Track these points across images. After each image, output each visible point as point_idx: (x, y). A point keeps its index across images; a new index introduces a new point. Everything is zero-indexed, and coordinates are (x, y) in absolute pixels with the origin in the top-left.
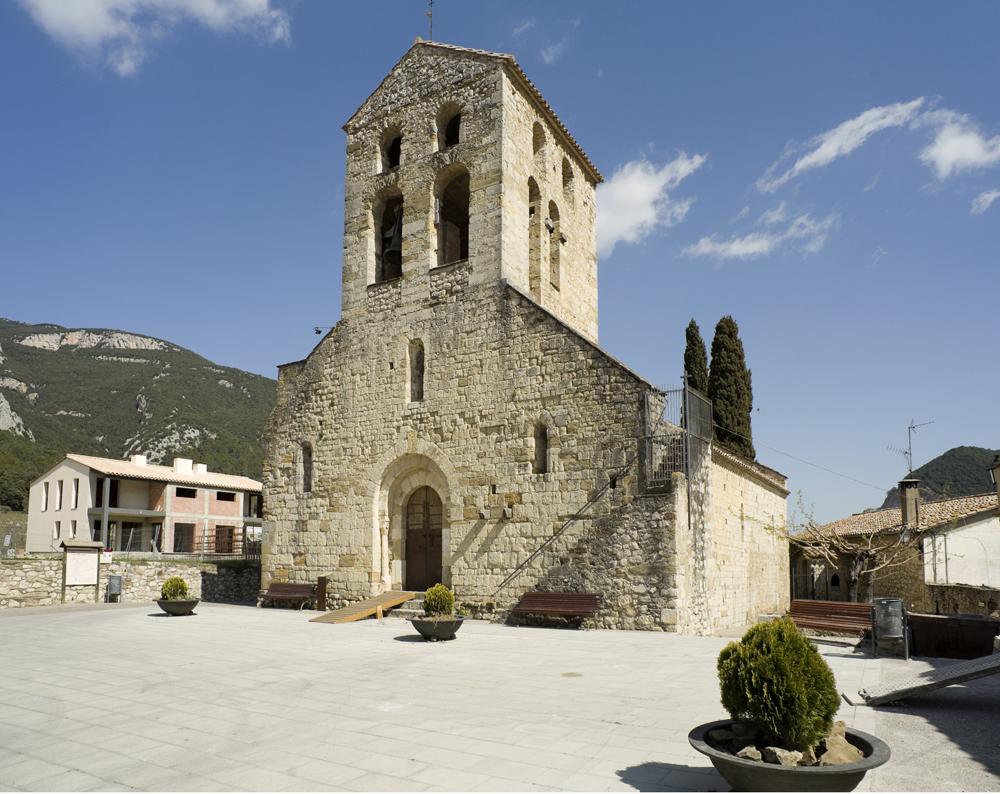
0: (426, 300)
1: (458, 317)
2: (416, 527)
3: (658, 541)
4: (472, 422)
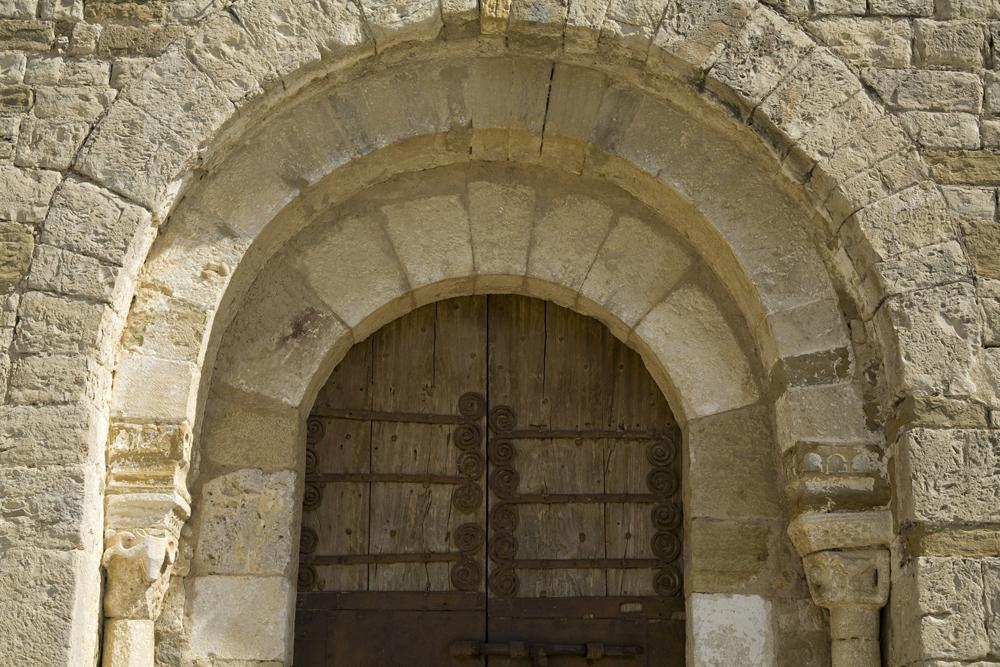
2: (386, 578)
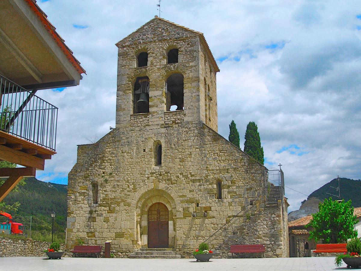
0: (162, 125)
1: (179, 134)
2: (153, 220)
3: (274, 225)
4: (186, 177)
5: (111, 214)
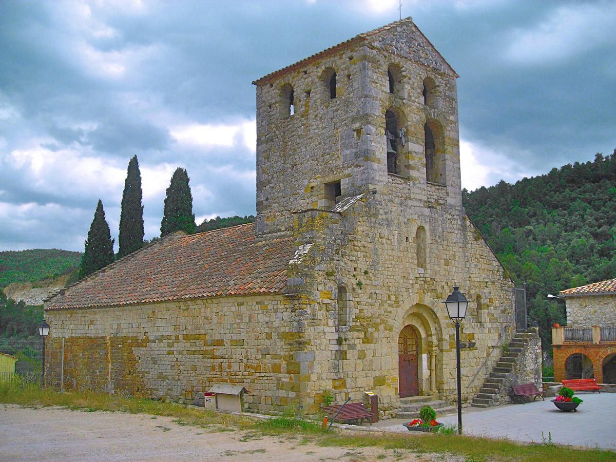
0: (425, 202)
5: (368, 346)
